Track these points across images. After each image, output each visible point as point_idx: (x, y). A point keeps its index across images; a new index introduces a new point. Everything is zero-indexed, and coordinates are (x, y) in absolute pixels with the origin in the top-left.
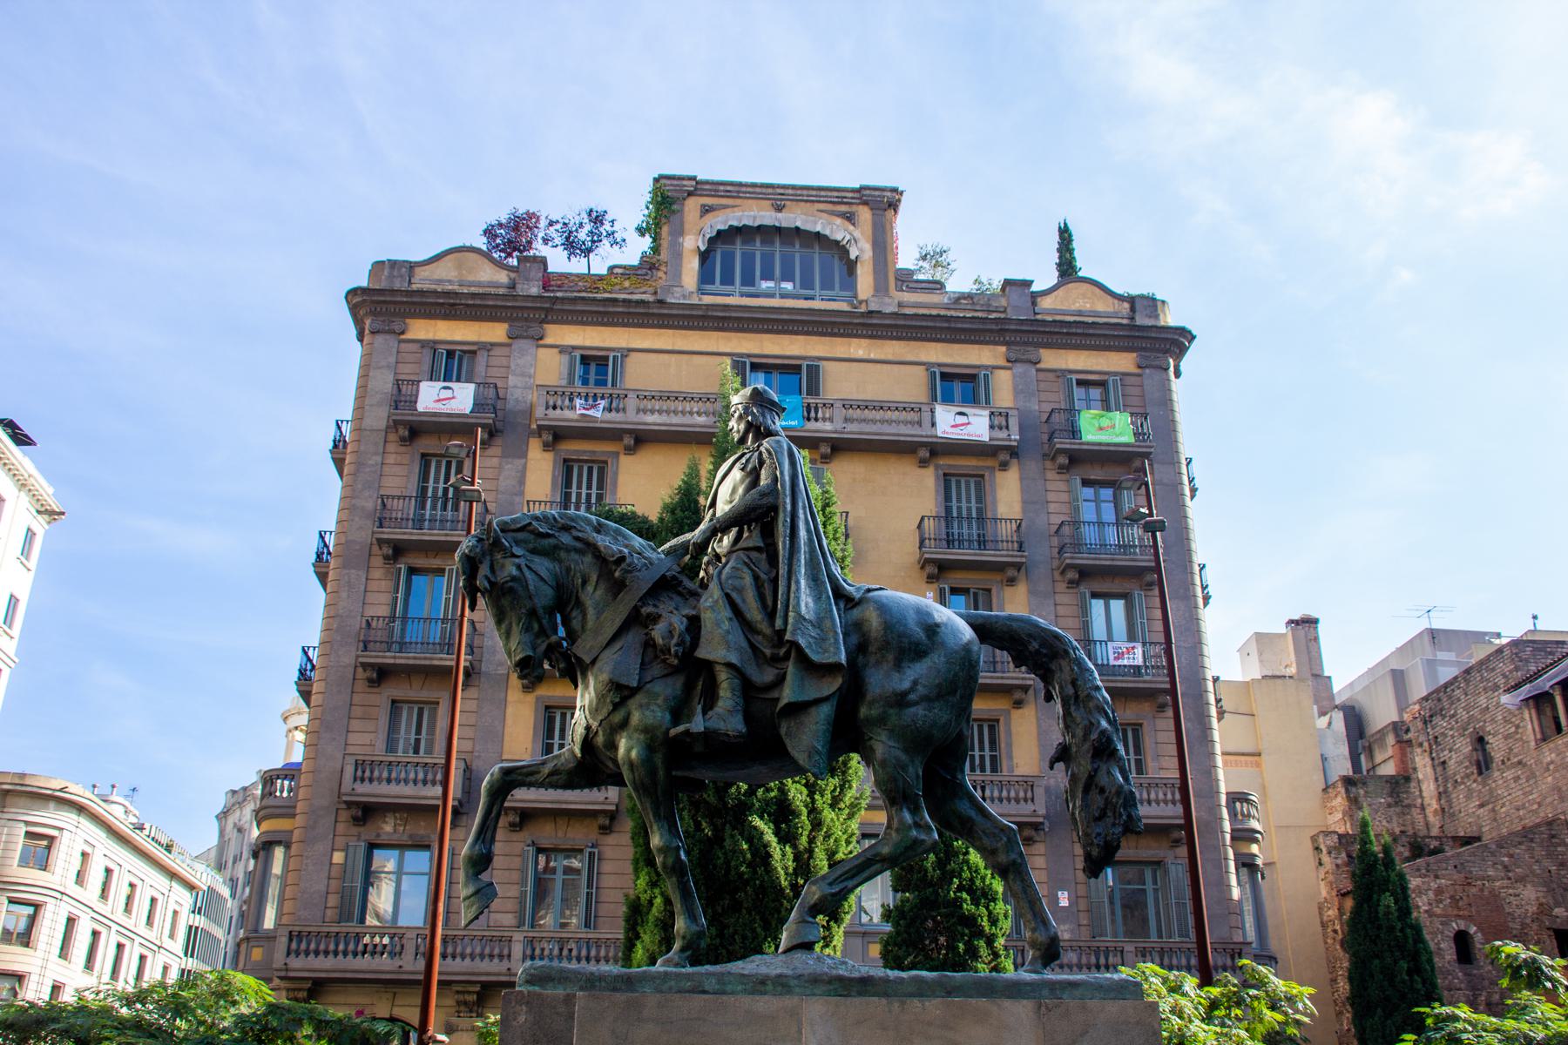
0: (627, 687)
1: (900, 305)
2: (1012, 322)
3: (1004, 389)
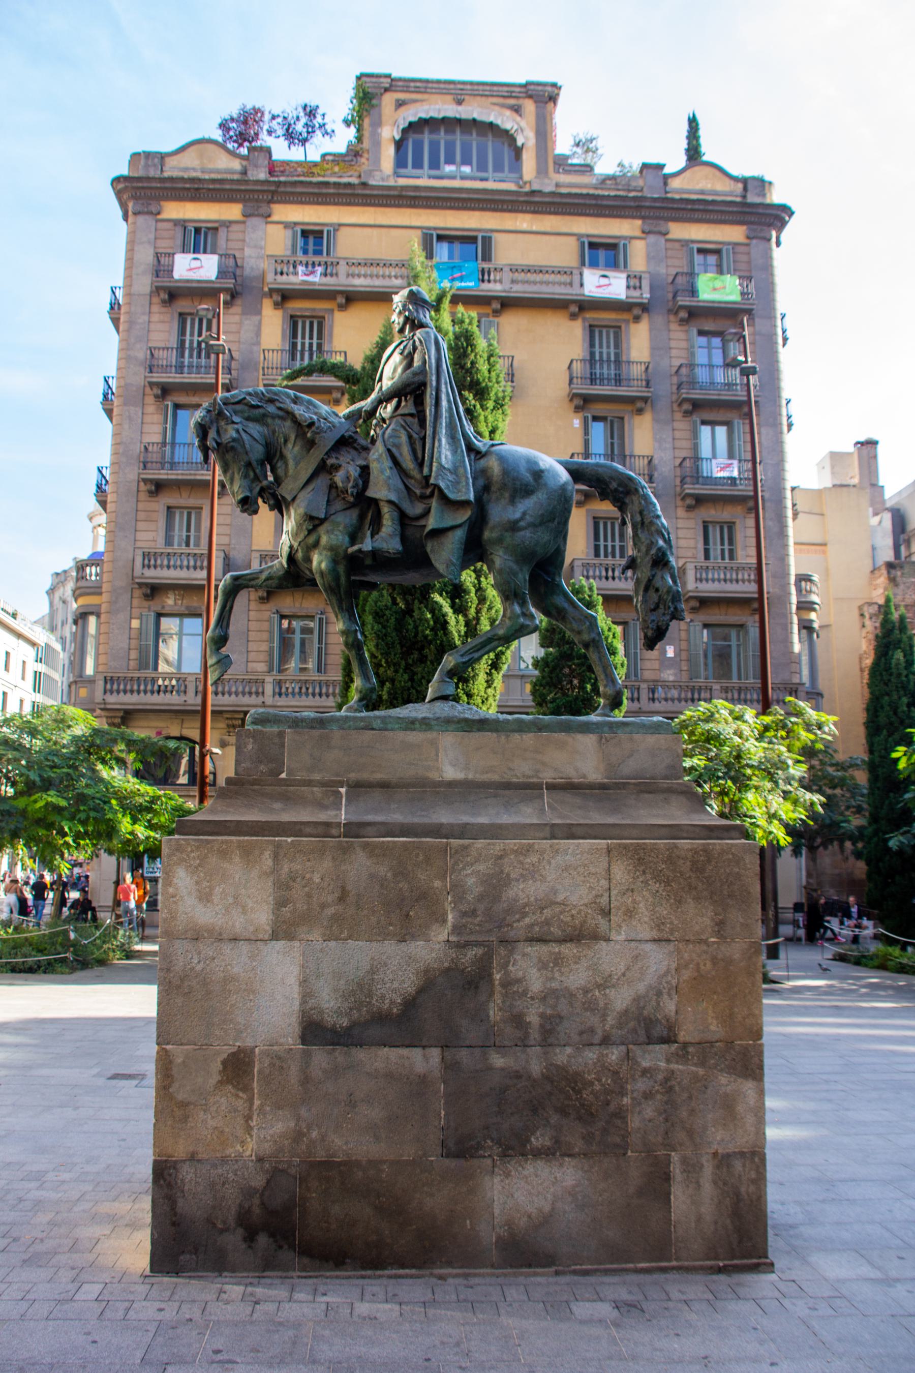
0: (317, 518)
1: (557, 185)
2: (648, 201)
3: (639, 255)
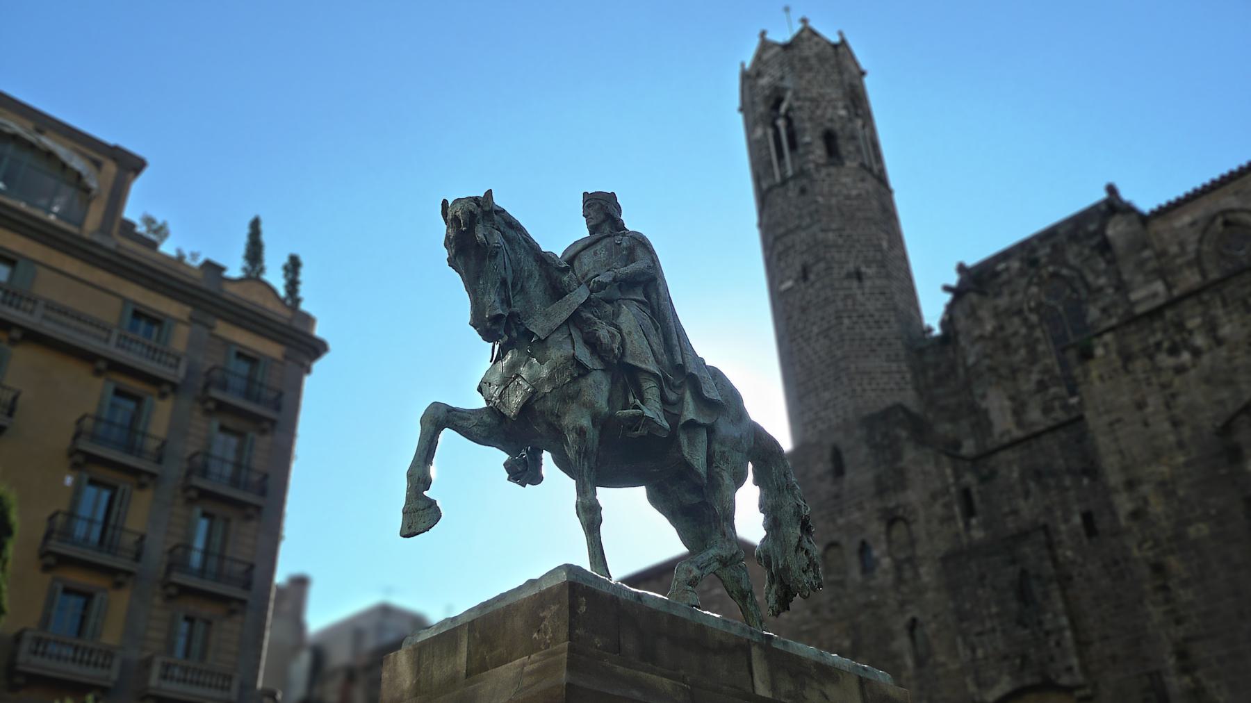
1: (119, 246)
2: (202, 291)
3: (180, 339)
